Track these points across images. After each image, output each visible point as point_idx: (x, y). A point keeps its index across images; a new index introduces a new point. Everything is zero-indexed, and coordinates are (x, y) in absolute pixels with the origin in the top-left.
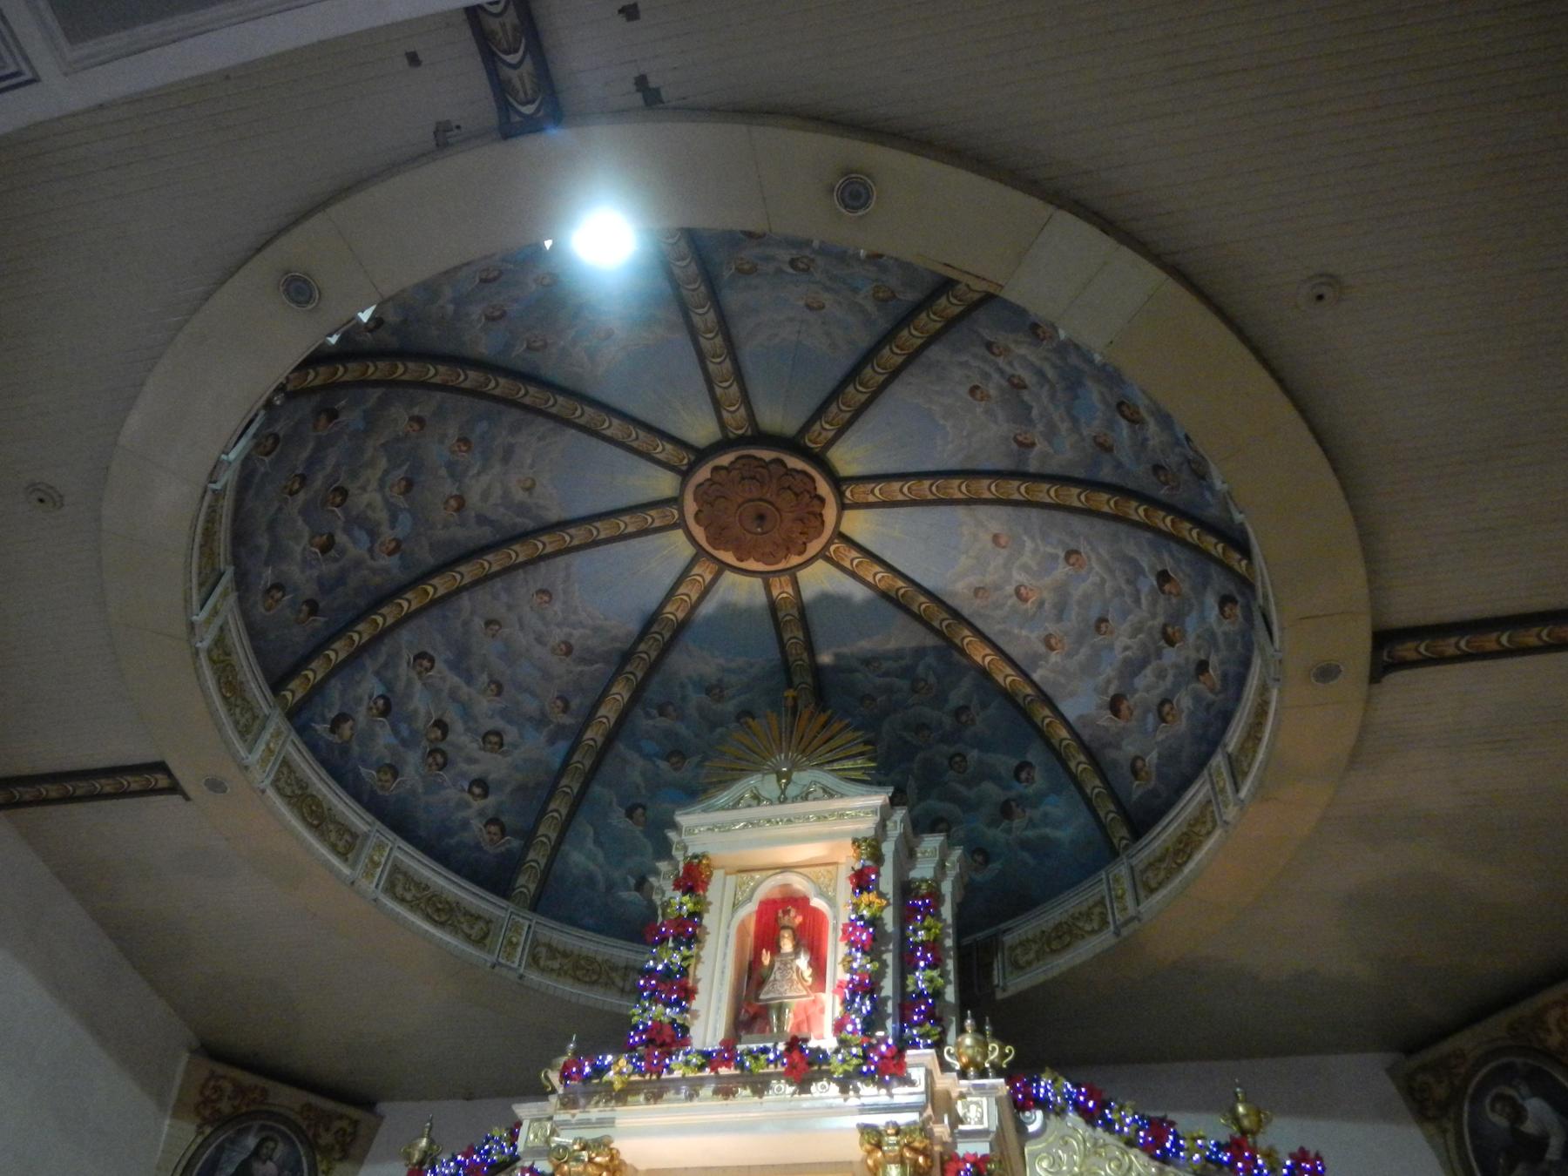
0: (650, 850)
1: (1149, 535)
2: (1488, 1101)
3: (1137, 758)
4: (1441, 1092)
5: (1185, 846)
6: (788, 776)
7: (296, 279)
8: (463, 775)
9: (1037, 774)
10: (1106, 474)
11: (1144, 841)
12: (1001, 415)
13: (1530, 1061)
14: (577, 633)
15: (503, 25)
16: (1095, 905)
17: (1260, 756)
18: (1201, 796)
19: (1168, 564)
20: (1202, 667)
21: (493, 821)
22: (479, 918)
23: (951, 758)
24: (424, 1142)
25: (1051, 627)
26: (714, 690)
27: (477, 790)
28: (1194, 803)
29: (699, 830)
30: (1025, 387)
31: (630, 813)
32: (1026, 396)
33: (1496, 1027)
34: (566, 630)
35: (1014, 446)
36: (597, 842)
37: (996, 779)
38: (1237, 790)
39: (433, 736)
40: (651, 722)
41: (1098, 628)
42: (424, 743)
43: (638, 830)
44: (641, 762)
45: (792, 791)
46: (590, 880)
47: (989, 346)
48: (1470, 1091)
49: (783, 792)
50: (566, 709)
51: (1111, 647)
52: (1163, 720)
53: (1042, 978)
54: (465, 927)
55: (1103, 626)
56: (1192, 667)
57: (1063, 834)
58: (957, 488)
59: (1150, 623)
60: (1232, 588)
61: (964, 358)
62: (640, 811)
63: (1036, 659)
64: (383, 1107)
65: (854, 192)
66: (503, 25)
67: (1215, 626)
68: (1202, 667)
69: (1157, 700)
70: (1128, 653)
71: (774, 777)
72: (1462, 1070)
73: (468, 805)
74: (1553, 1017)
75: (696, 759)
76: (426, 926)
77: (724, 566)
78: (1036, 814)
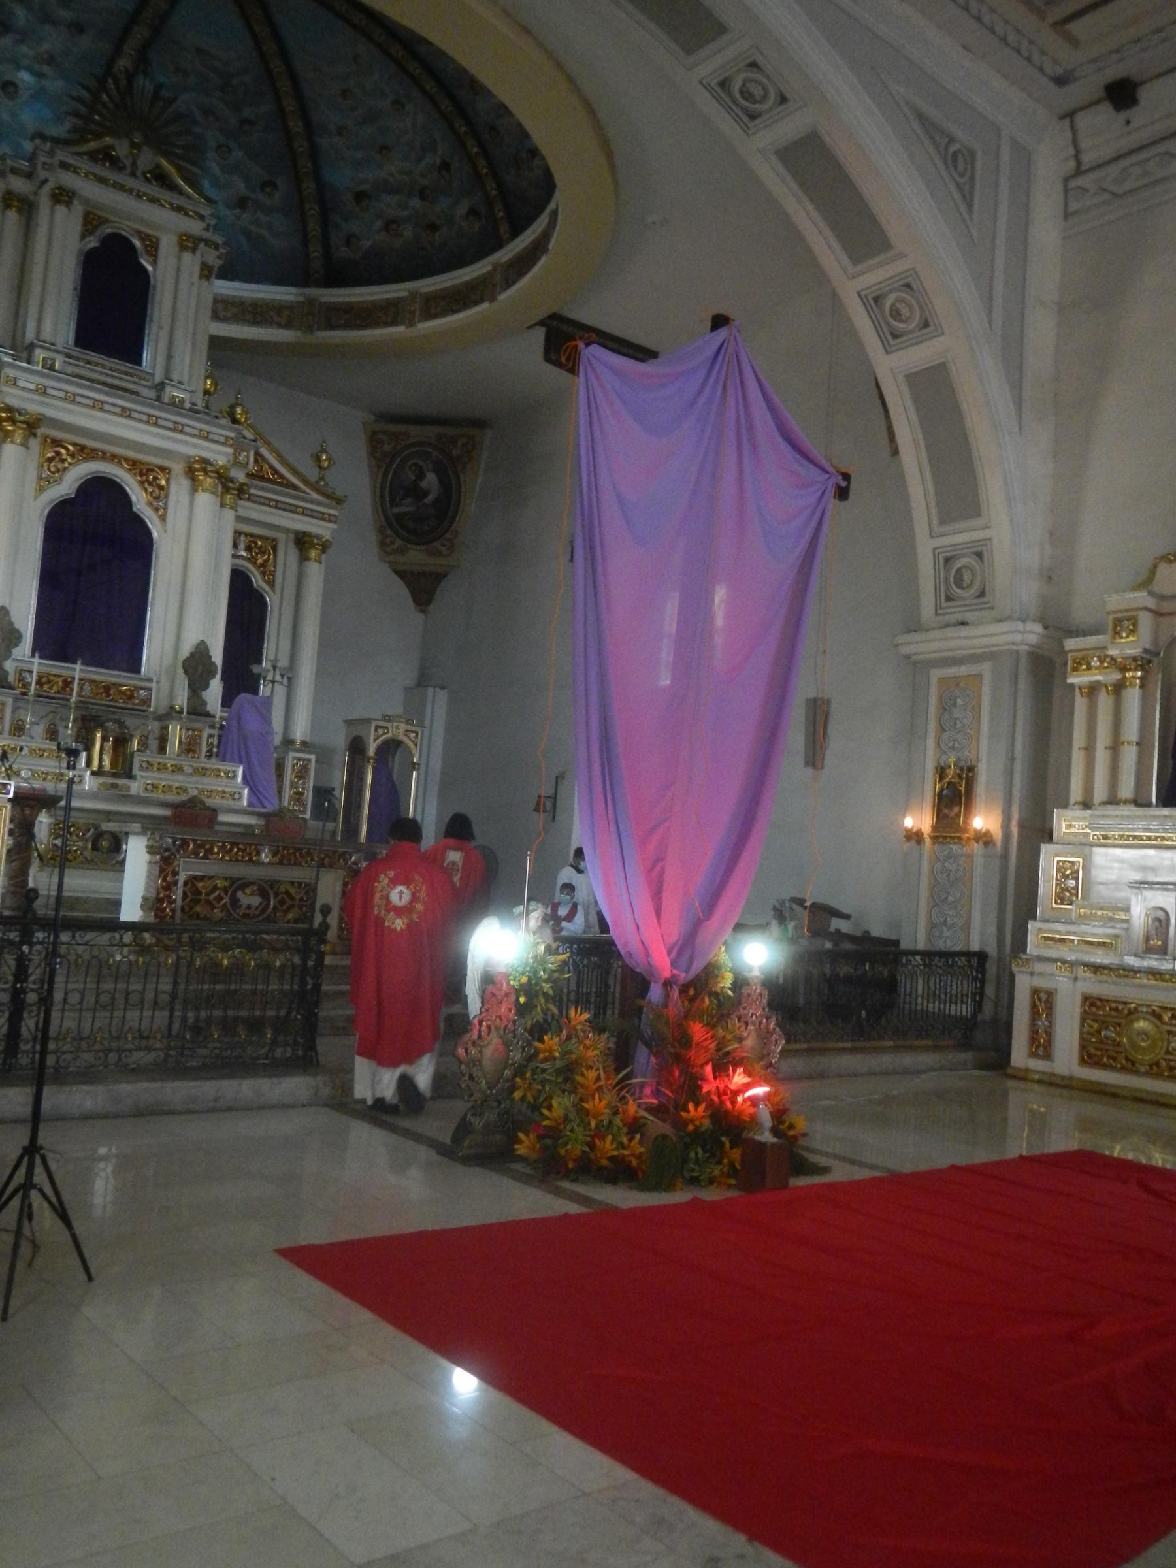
4: (387, 448)
5: (364, 316)
20: (433, 227)
33: (431, 432)
68: (433, 227)
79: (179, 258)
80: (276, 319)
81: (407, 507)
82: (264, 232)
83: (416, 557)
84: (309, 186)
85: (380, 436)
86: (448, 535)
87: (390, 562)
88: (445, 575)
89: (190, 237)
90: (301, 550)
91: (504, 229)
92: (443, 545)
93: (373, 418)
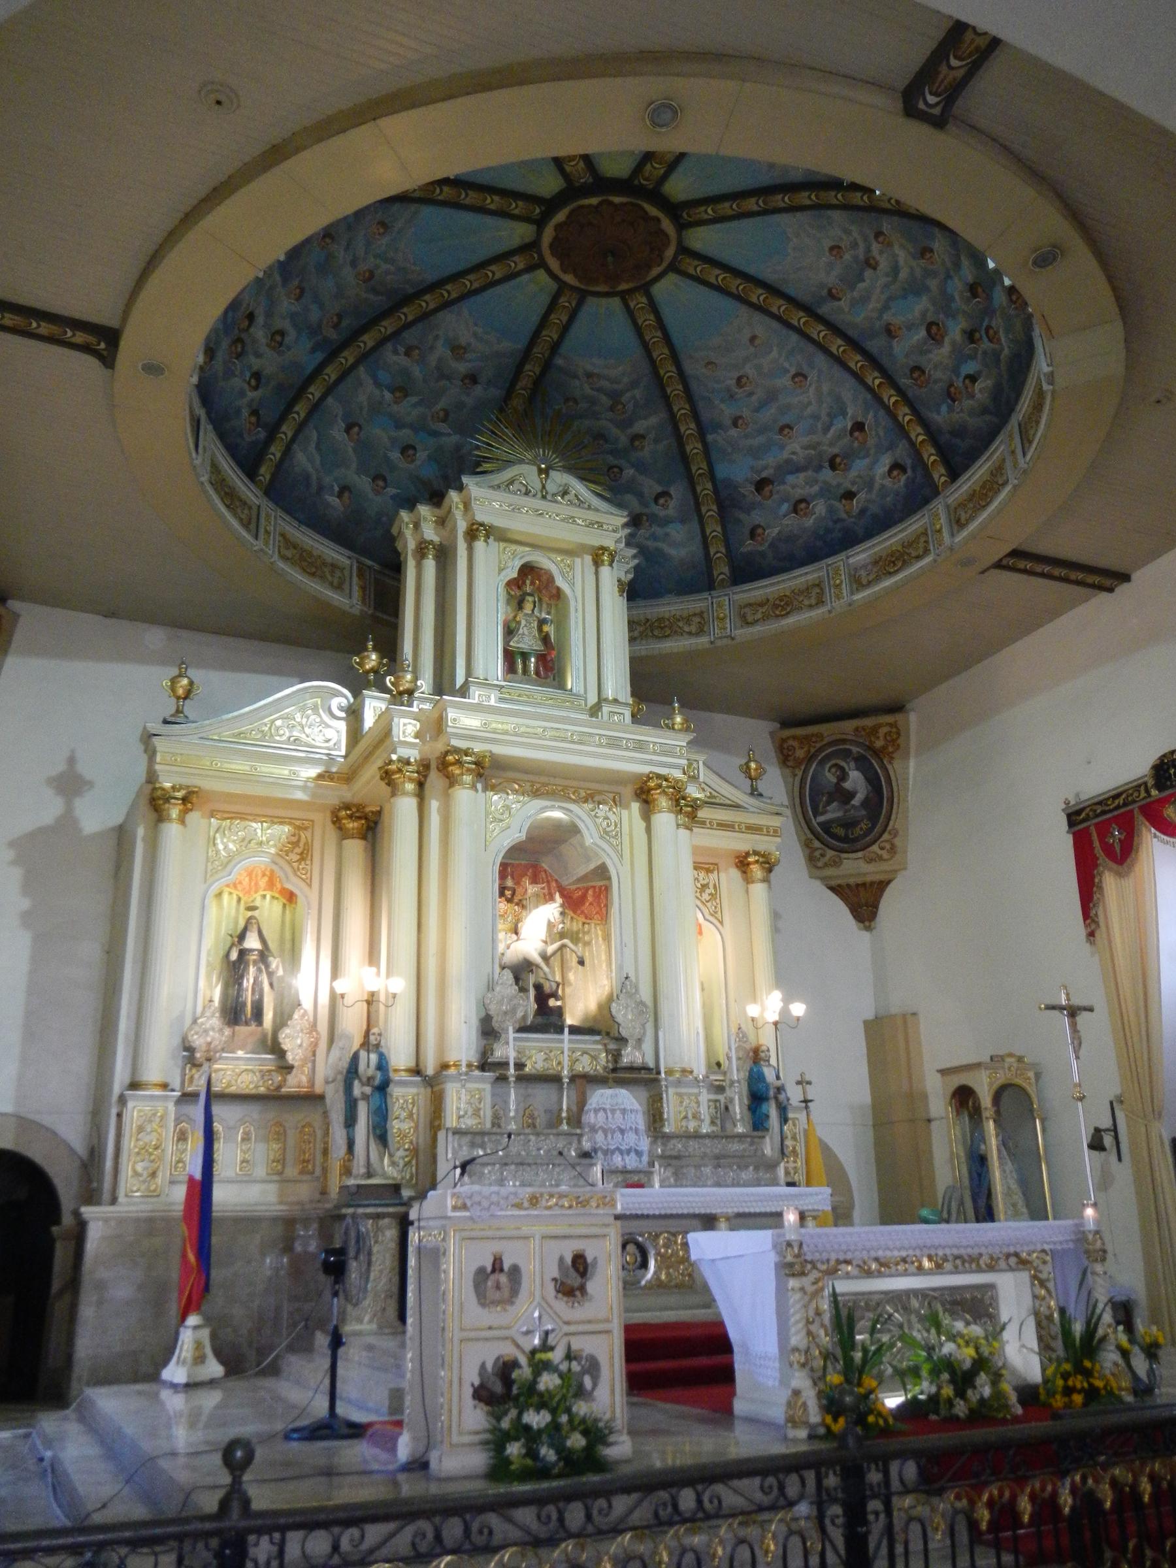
0: (354, 466)
1: (869, 396)
2: (828, 766)
3: (759, 526)
4: (800, 753)
5: (784, 605)
6: (546, 472)
7: (670, 106)
8: (250, 367)
9: (672, 504)
10: (874, 345)
11: (746, 587)
12: (834, 273)
14: (385, 266)
15: (973, 41)
16: (695, 615)
17: (887, 583)
18: (810, 577)
19: (869, 420)
20: (849, 495)
21: (255, 413)
22: (245, 503)
23: (611, 468)
24: (185, 681)
25: (746, 413)
26: (458, 350)
27: (253, 382)
30: (875, 269)
31: (348, 430)
32: (868, 273)
34: (378, 261)
35: (824, 292)
36: (318, 448)
37: (640, 495)
38: (852, 593)
39: (242, 326)
40: (395, 358)
41: (782, 429)
42: (236, 331)
43: (349, 448)
44: (369, 387)
45: (551, 487)
46: (307, 477)
47: (878, 234)
49: (544, 487)
50: (336, 326)
51: (782, 447)
52: (795, 511)
53: (643, 653)
54: (239, 511)
55: (786, 431)
56: (842, 491)
57: (673, 552)
58: (757, 295)
59: (825, 448)
60: (908, 462)
61: (853, 228)
62: (356, 429)
63: (718, 426)
64: (14, 605)
65: (1045, 259)
66: (973, 41)
67: (877, 478)
68: (849, 495)
69: (797, 497)
70: (794, 457)
71: (535, 468)
72: (818, 745)
73: (242, 394)
74: (883, 731)
75: (414, 399)
76: (223, 509)
77: (542, 264)
78: (659, 531)
79: (597, 573)
80: (686, 629)
81: (833, 812)
82: (660, 545)
83: (854, 867)
84: (705, 488)
85: (791, 742)
86: (886, 836)
87: (823, 879)
88: (889, 882)
89: (604, 549)
90: (744, 872)
91: (939, 474)
92: (882, 848)
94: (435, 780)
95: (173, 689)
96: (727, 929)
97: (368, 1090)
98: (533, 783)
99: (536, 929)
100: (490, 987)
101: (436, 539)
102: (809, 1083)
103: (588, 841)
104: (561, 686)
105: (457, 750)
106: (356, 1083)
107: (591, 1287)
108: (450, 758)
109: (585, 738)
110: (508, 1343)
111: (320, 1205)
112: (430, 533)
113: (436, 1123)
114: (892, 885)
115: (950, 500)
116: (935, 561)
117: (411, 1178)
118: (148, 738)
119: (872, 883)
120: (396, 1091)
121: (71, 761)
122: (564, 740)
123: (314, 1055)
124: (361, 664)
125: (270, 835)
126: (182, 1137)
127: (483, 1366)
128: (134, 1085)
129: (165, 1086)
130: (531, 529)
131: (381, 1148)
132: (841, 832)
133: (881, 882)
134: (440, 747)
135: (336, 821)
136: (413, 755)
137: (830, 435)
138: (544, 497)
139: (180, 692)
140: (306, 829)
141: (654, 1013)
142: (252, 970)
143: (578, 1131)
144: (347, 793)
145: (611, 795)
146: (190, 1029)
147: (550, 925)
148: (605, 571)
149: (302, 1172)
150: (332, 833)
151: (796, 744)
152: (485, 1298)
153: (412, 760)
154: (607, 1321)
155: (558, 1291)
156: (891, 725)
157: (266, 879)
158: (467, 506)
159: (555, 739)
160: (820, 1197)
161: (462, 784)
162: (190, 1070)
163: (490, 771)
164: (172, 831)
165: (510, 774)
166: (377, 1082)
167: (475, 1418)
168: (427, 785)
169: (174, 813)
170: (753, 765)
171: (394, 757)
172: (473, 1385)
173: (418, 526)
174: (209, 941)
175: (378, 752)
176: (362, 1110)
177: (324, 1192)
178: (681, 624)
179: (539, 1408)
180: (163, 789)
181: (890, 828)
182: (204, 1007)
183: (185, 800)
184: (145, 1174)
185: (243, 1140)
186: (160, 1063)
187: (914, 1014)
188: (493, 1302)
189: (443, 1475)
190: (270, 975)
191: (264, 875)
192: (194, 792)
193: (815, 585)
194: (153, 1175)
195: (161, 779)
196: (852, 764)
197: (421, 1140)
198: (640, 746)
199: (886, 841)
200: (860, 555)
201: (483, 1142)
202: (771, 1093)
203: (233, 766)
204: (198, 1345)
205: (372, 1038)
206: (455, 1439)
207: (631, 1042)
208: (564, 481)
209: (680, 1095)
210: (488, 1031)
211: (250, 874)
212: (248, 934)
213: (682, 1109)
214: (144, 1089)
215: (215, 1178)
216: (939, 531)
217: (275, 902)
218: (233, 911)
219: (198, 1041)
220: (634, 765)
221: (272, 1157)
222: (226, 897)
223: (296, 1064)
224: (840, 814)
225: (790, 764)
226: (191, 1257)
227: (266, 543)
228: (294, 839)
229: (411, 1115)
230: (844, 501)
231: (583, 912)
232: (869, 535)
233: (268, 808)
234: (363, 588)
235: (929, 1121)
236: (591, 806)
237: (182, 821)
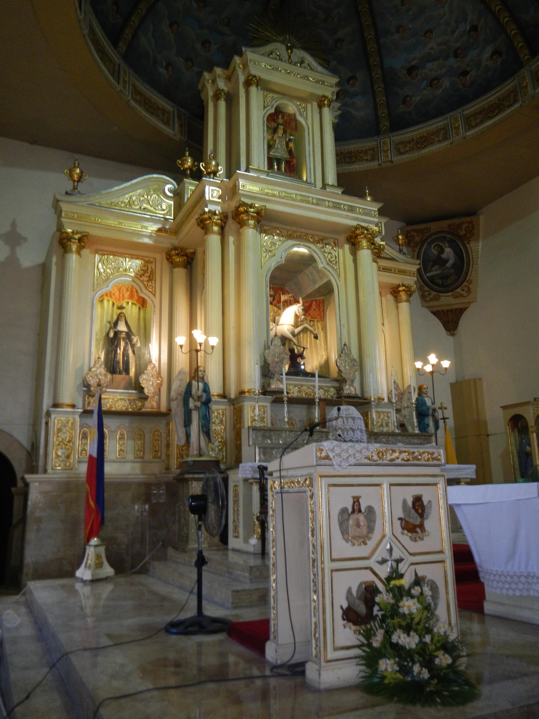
4: (417, 239)
5: (423, 142)
13: (450, 236)
16: (370, 149)
20: (465, 73)
24: (78, 171)
28: (435, 126)
29: (257, 62)
31: (171, 26)
33: (444, 224)
38: (466, 132)
41: (426, 33)
45: (294, 58)
48: (428, 241)
49: (290, 57)
62: (176, 26)
68: (465, 73)
71: (284, 47)
72: (427, 235)
79: (321, 113)
81: (435, 271)
83: (447, 301)
85: (412, 233)
86: (465, 283)
87: (428, 308)
88: (466, 309)
89: (325, 97)
90: (396, 297)
92: (463, 290)
93: (404, 224)
94: (231, 224)
95: (71, 176)
96: (386, 328)
97: (198, 404)
98: (288, 231)
99: (288, 318)
100: (267, 347)
101: (226, 89)
102: (446, 408)
103: (320, 266)
104: (300, 178)
105: (245, 204)
106: (191, 400)
107: (428, 524)
108: (241, 209)
109: (320, 202)
110: (368, 572)
111: (166, 475)
112: (222, 85)
113: (238, 426)
114: (467, 310)
115: (533, 68)
116: (521, 106)
117: (223, 458)
118: (56, 204)
119: (456, 309)
120: (214, 407)
121: (14, 225)
122: (308, 202)
123: (160, 391)
124: (182, 164)
125: (132, 265)
126: (84, 436)
127: (349, 591)
128: (56, 405)
129: (73, 406)
130: (282, 84)
131: (207, 440)
132: (439, 281)
133: (461, 309)
134: (234, 204)
135: (169, 258)
136: (218, 209)
137: (455, 36)
138: (291, 63)
139: (76, 177)
140: (151, 263)
141: (360, 365)
142: (122, 344)
143: (325, 430)
144: (175, 241)
145: (333, 240)
146: (87, 374)
147: (296, 316)
148: (326, 111)
149: (154, 457)
150: (166, 265)
151: (415, 234)
152: (348, 534)
153: (217, 212)
154: (441, 552)
155: (403, 528)
156: (469, 222)
157: (129, 293)
158: (245, 66)
159: (302, 201)
160: (470, 470)
161: (248, 225)
162: (88, 398)
163: (265, 220)
164: (73, 259)
165: (275, 224)
166: (204, 399)
167: (347, 635)
168: (227, 228)
169: (74, 247)
170: (400, 237)
171: (207, 210)
172: (342, 607)
173: (214, 81)
174: (97, 327)
175: (196, 209)
176: (195, 417)
177: (168, 468)
178: (361, 155)
179: (408, 629)
180: (67, 233)
181: (468, 279)
182: (95, 362)
183: (80, 240)
184: (63, 456)
185: (120, 438)
186: (69, 392)
187: (480, 379)
188: (354, 538)
189: (322, 687)
190: (133, 346)
191: (127, 290)
192: (85, 236)
193: (441, 129)
194: (68, 457)
195: (65, 227)
196: (447, 245)
197: (228, 437)
198: (352, 209)
199: (465, 286)
200: (471, 109)
201: (271, 435)
202: (431, 412)
203: (108, 222)
204: (98, 556)
205: (200, 373)
206: (331, 654)
207: (349, 382)
208: (301, 56)
209: (377, 412)
210: (267, 372)
211: (119, 290)
212: (119, 322)
213: (380, 420)
214: (63, 408)
215: (105, 460)
216: (526, 86)
217: (134, 306)
218: (110, 311)
219: (93, 382)
220: (347, 220)
221: (137, 449)
222: (105, 302)
223: (150, 395)
224: (438, 272)
225: (411, 245)
226: (92, 504)
227: (125, 88)
228: (145, 268)
229: (221, 422)
230: (461, 77)
231: (310, 314)
232: (476, 96)
233: (129, 248)
234: (181, 126)
235: (488, 435)
236: (321, 246)
237: (79, 253)
